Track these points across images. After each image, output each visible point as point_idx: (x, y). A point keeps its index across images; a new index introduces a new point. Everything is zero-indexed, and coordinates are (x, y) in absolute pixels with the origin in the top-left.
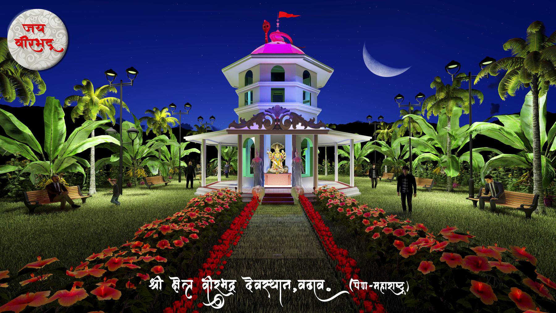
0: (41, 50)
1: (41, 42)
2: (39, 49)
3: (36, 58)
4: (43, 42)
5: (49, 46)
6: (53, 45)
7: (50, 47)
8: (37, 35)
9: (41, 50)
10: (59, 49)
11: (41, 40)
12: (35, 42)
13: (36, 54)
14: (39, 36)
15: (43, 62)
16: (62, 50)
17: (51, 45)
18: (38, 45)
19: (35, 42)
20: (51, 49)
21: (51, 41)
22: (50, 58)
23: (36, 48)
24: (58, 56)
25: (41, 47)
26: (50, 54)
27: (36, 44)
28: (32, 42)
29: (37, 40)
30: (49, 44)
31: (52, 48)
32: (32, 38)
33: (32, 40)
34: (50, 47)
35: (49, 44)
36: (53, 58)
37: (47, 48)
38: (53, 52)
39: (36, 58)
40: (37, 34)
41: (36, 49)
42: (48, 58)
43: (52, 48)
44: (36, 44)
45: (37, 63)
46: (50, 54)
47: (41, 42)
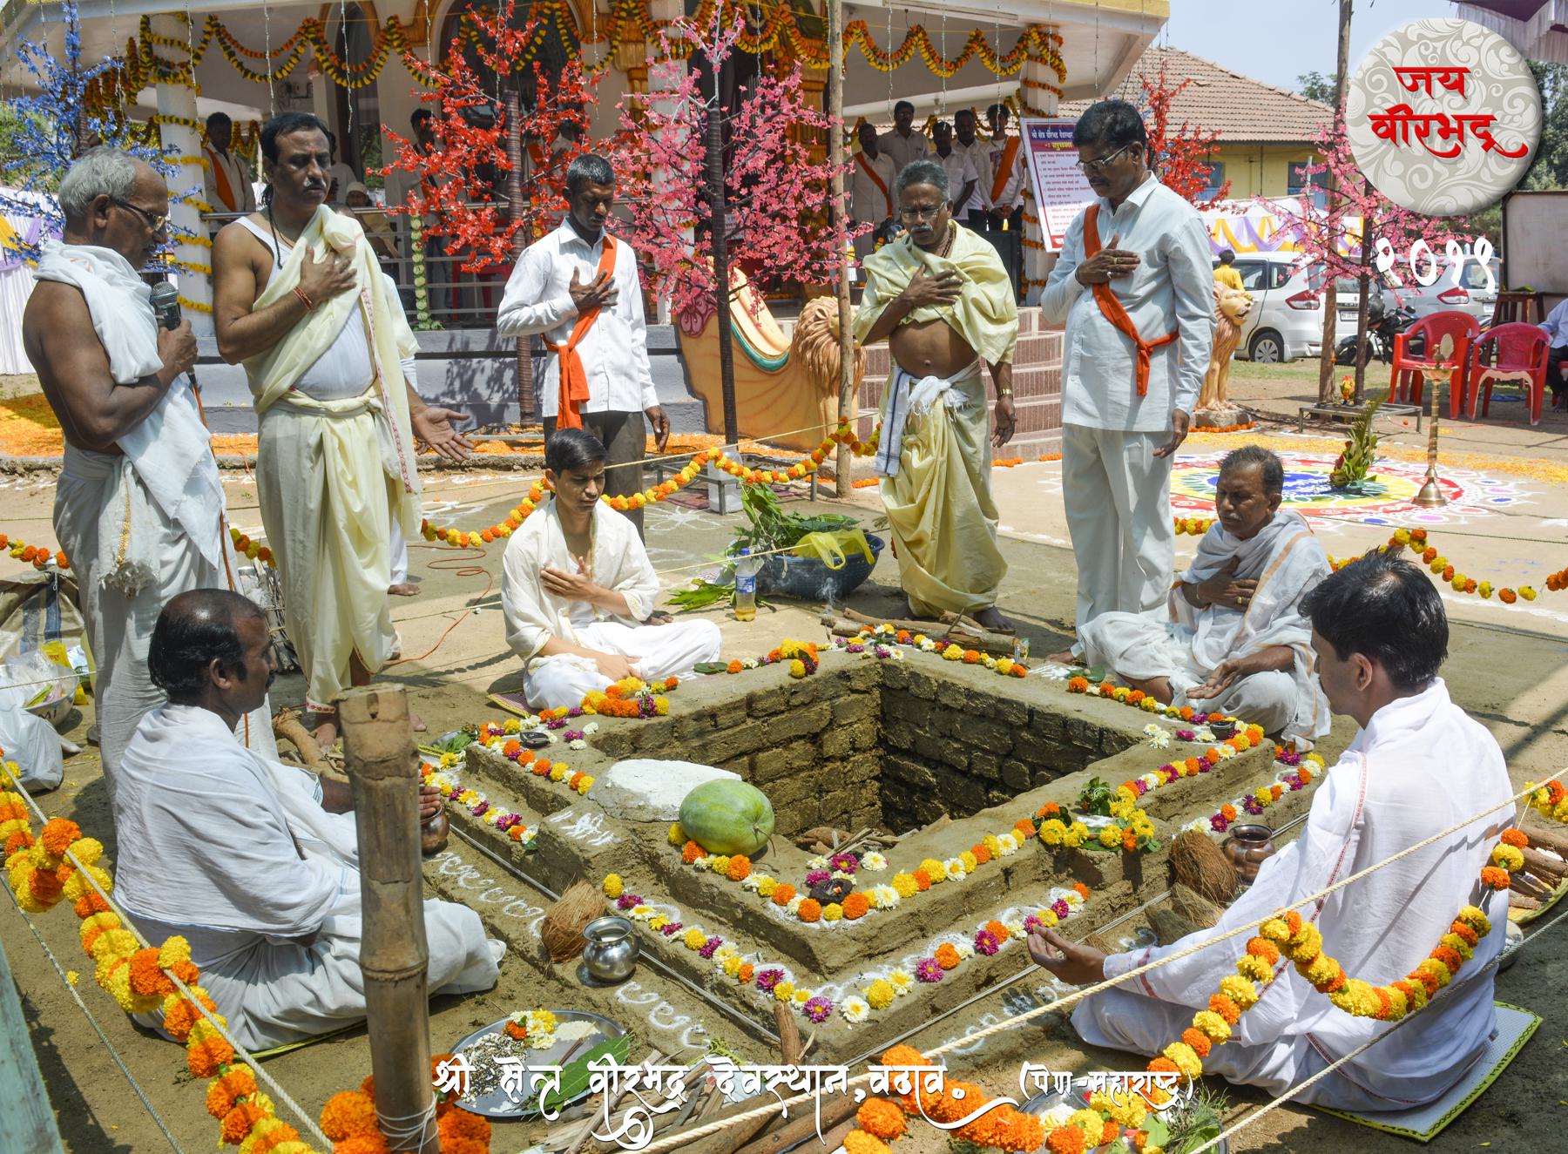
0: (1456, 152)
1: (1454, 125)
2: (1450, 148)
3: (1437, 175)
8: (1438, 102)
9: (1456, 152)
11: (1459, 118)
12: (1435, 126)
13: (1438, 164)
14: (1443, 102)
15: (1462, 189)
18: (1445, 133)
19: (1435, 126)
23: (1438, 143)
25: (1454, 141)
27: (1440, 132)
28: (1427, 126)
29: (1441, 118)
32: (1426, 112)
33: (1427, 119)
39: (1437, 175)
44: (1440, 132)
45: (1442, 193)
47: (1454, 125)
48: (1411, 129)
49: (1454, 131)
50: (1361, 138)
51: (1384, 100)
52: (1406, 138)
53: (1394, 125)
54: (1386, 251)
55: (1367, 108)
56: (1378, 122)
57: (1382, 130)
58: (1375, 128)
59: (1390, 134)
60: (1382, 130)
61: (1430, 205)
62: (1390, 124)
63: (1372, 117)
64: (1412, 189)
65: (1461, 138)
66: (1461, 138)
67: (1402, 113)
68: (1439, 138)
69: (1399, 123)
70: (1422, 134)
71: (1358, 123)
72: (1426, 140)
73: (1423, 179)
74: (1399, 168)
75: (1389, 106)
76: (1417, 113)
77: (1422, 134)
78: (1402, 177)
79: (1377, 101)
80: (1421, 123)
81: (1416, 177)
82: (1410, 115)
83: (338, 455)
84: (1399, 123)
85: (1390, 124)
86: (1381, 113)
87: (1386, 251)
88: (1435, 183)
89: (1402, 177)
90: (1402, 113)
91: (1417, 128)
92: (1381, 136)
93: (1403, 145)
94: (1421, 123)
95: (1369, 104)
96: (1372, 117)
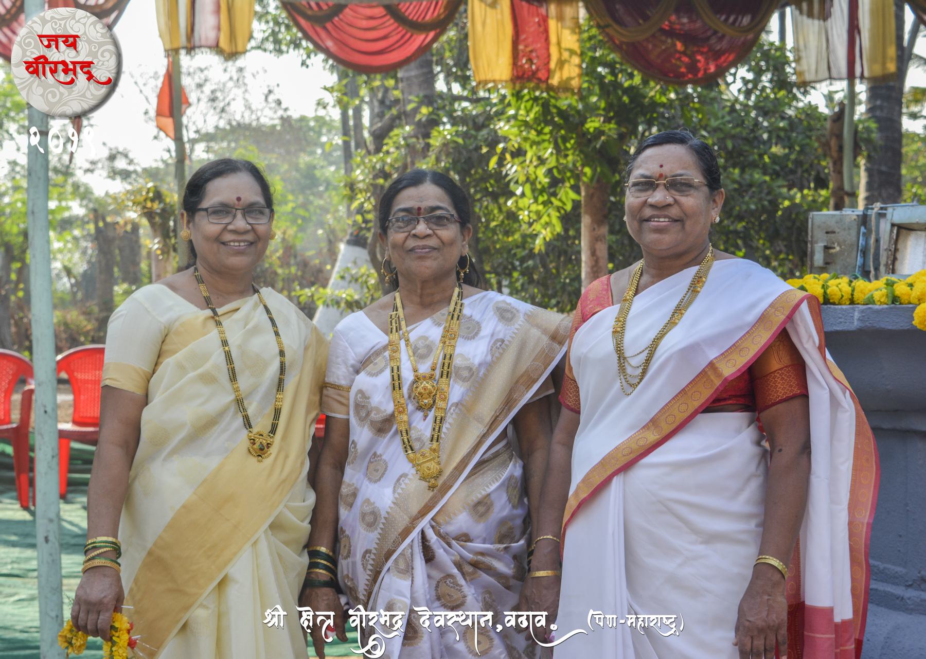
0: (72, 81)
1: (71, 66)
2: (69, 80)
3: (61, 94)
4: (75, 67)
5: (85, 73)
6: (94, 72)
7: (87, 76)
9: (72, 81)
10: (104, 80)
11: (72, 62)
12: (60, 67)
13: (62, 88)
15: (75, 102)
16: (110, 80)
17: (89, 73)
18: (66, 71)
19: (60, 67)
20: (89, 79)
21: (89, 64)
22: (88, 95)
23: (62, 77)
24: (104, 90)
26: (88, 88)
27: (63, 70)
29: (64, 63)
30: (85, 70)
31: (90, 77)
34: (87, 76)
35: (85, 70)
36: (92, 94)
37: (82, 77)
38: (92, 85)
39: (61, 94)
41: (62, 80)
42: (84, 95)
43: (90, 77)
44: (63, 70)
45: (64, 105)
46: (88, 88)
47: (71, 66)
49: (71, 70)
65: (75, 74)
66: (75, 74)
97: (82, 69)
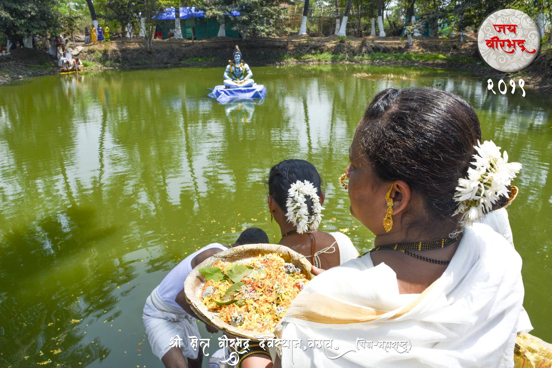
0: (513, 51)
1: (512, 43)
2: (511, 50)
3: (507, 59)
4: (514, 43)
9: (513, 51)
11: (514, 41)
12: (506, 43)
13: (507, 55)
18: (509, 46)
19: (506, 43)
23: (507, 49)
27: (508, 45)
29: (508, 41)
32: (503, 39)
33: (504, 41)
37: (518, 49)
39: (507, 59)
40: (508, 35)
44: (508, 45)
45: (509, 65)
47: (512, 43)
48: (499, 44)
49: (512, 45)
50: (483, 48)
51: (490, 35)
52: (497, 47)
53: (493, 43)
54: (491, 83)
55: (485, 38)
56: (488, 42)
57: (489, 45)
58: (487, 44)
59: (492, 46)
60: (489, 45)
61: (504, 69)
62: (492, 43)
63: (486, 41)
64: (499, 64)
65: (515, 47)
66: (515, 47)
67: (496, 39)
68: (507, 47)
69: (495, 42)
70: (502, 46)
71: (482, 42)
72: (503, 48)
73: (503, 60)
74: (495, 57)
75: (492, 37)
76: (501, 39)
77: (502, 46)
78: (496, 60)
79: (488, 35)
80: (502, 43)
81: (500, 60)
82: (498, 40)
83: (184, 154)
84: (495, 42)
85: (492, 43)
86: (489, 39)
87: (491, 83)
88: (506, 61)
89: (496, 60)
90: (496, 39)
91: (501, 44)
92: (489, 47)
93: (496, 49)
94: (502, 43)
95: (485, 36)
96: (486, 41)
97: (518, 44)
